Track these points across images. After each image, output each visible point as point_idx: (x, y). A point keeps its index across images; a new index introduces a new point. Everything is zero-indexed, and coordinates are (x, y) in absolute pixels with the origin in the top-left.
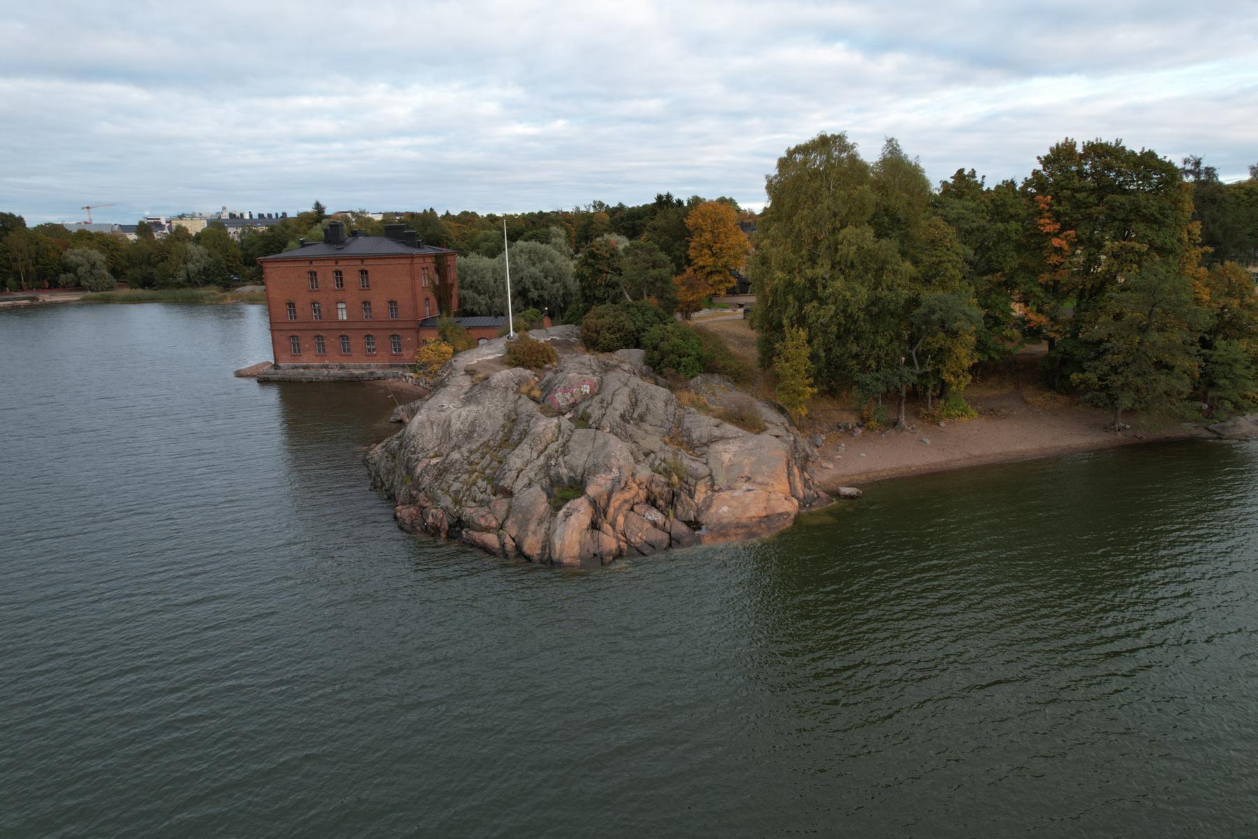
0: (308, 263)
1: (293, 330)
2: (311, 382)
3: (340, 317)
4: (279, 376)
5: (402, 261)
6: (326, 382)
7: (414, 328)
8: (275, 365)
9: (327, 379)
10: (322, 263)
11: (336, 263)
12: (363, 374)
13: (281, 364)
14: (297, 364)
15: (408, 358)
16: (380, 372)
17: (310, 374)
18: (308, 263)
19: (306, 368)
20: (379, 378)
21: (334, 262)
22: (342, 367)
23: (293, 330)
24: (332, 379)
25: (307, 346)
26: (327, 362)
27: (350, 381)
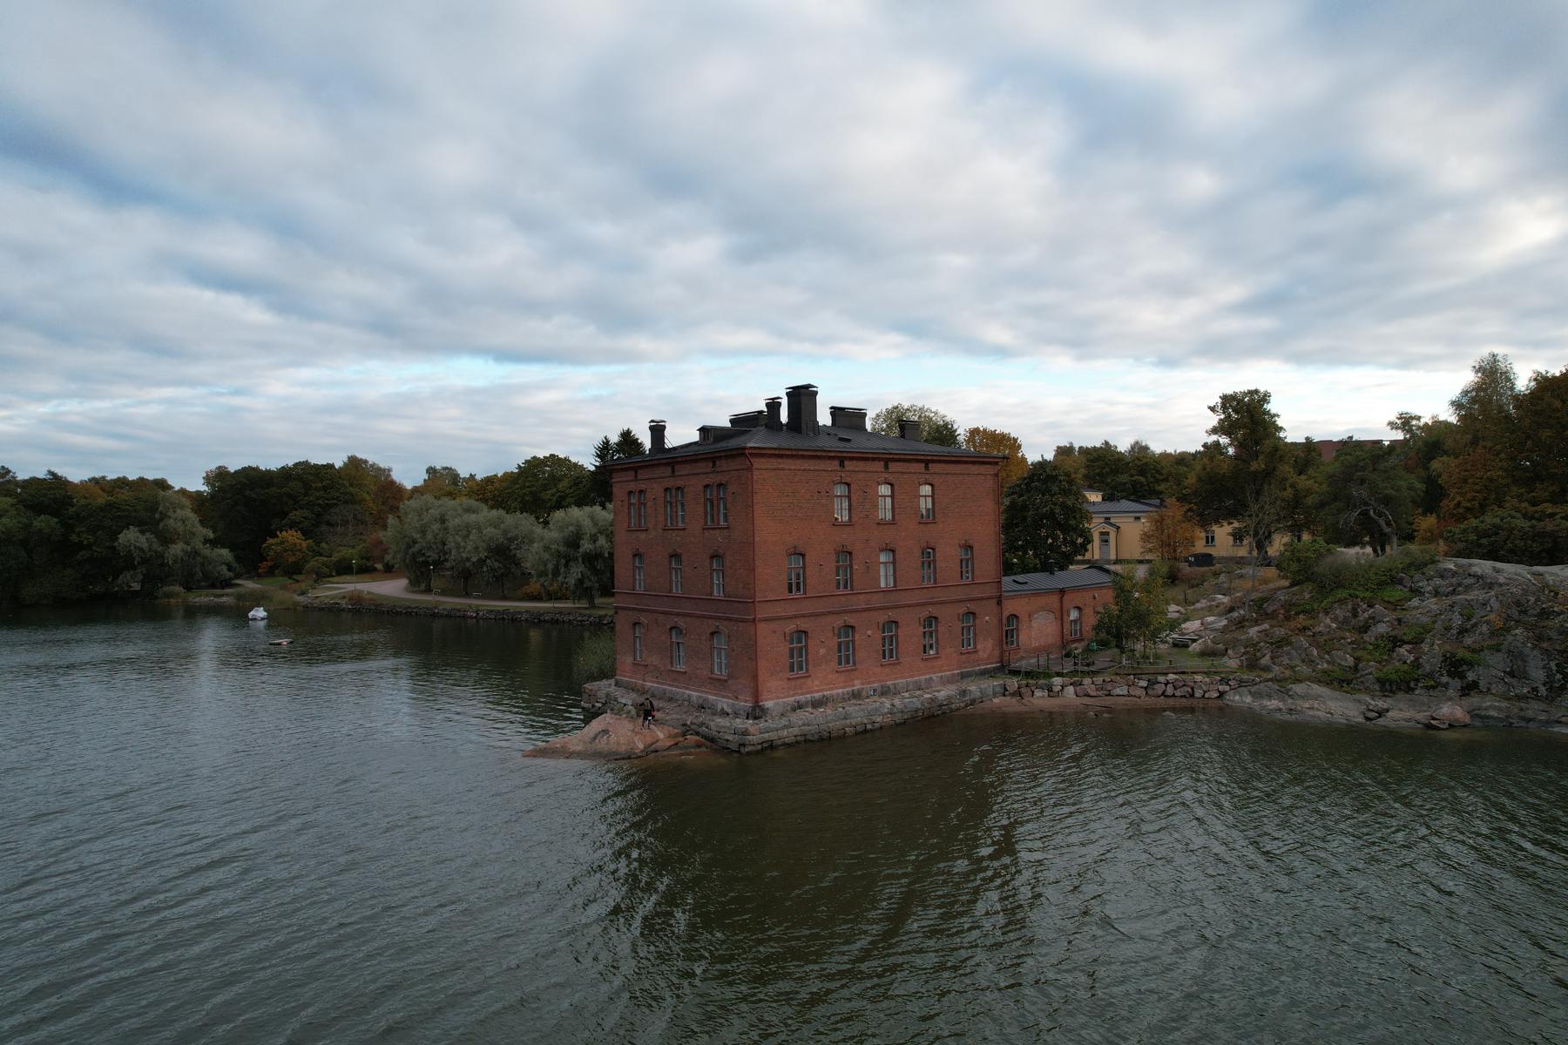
0: (836, 463)
1: (796, 617)
2: (866, 731)
3: (883, 585)
4: (796, 731)
5: (983, 469)
6: (891, 727)
7: (992, 598)
8: (754, 709)
9: (888, 720)
10: (860, 465)
11: (886, 467)
12: (949, 698)
13: (769, 704)
14: (802, 698)
15: (985, 656)
16: (974, 688)
17: (857, 714)
18: (836, 463)
19: (816, 704)
20: (973, 702)
21: (883, 463)
22: (885, 692)
23: (796, 617)
24: (898, 718)
25: (822, 651)
26: (857, 686)
27: (928, 718)
